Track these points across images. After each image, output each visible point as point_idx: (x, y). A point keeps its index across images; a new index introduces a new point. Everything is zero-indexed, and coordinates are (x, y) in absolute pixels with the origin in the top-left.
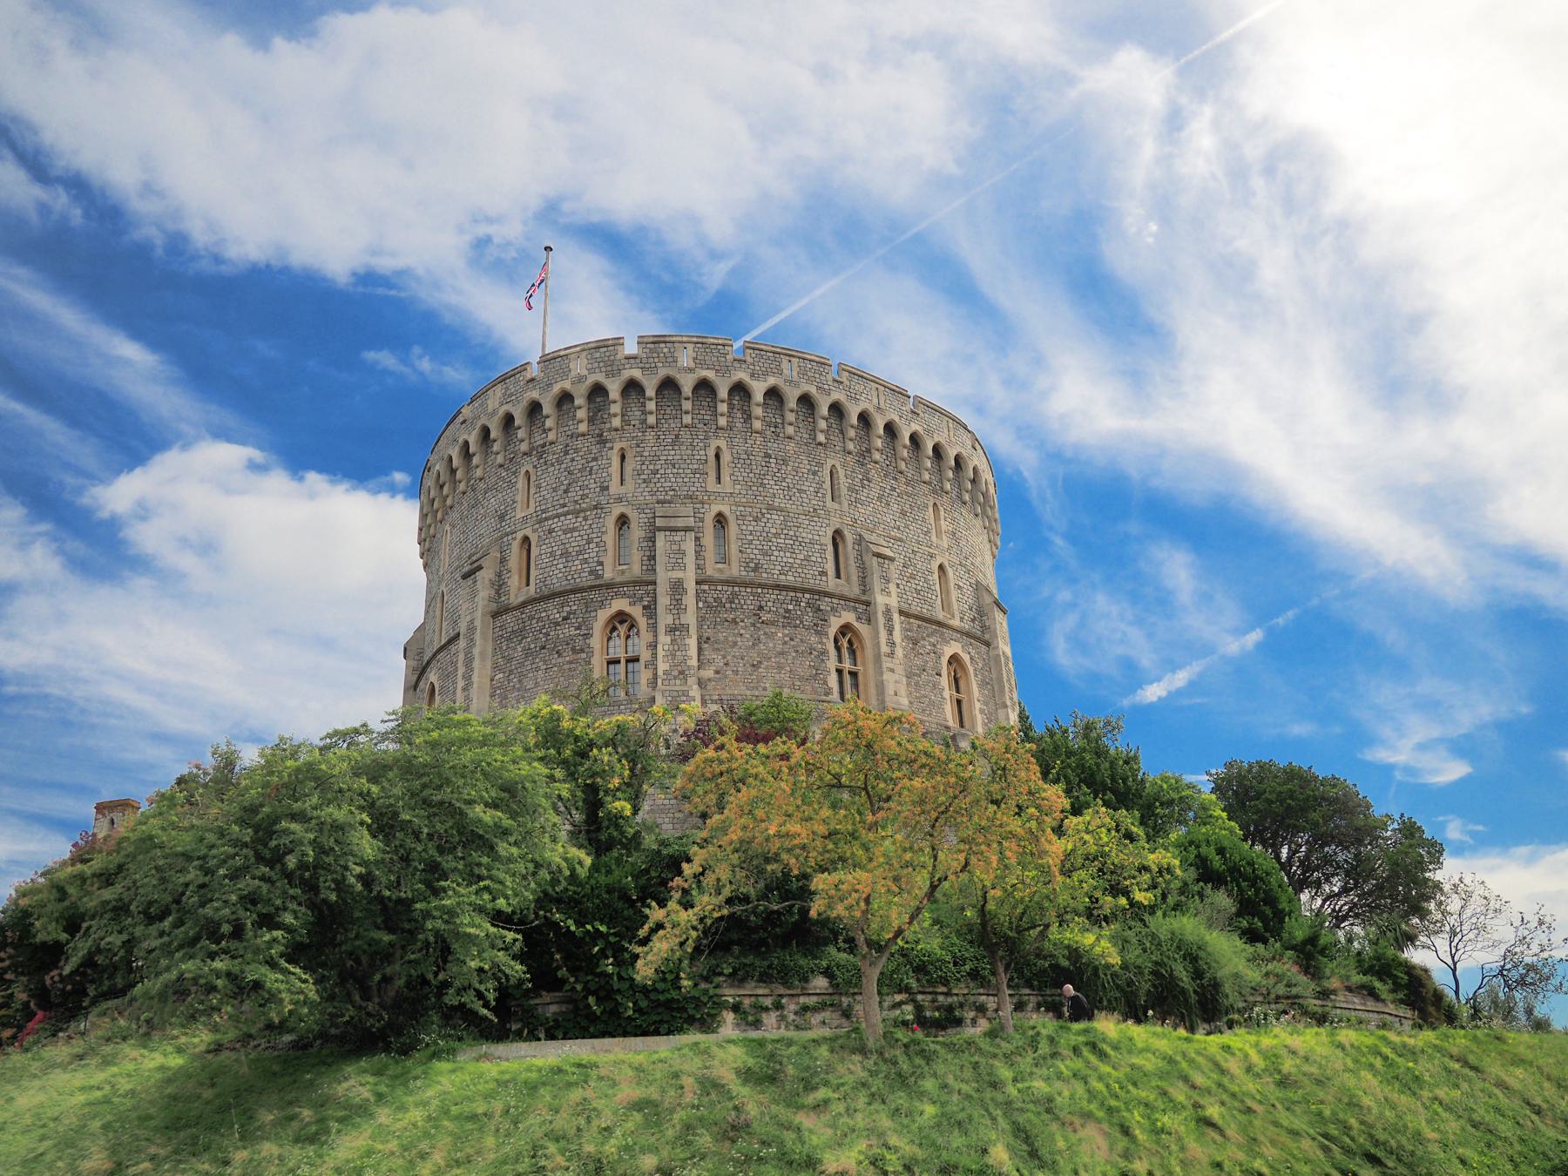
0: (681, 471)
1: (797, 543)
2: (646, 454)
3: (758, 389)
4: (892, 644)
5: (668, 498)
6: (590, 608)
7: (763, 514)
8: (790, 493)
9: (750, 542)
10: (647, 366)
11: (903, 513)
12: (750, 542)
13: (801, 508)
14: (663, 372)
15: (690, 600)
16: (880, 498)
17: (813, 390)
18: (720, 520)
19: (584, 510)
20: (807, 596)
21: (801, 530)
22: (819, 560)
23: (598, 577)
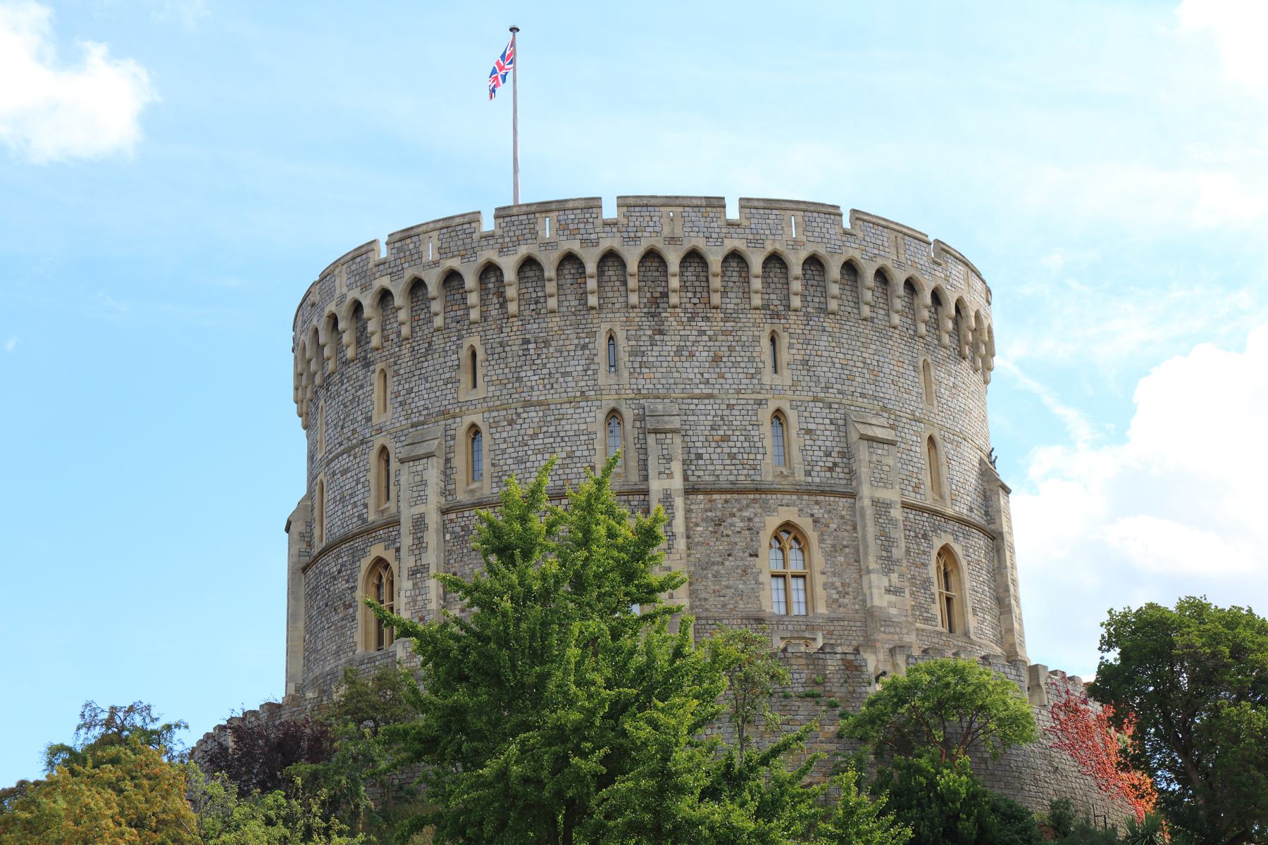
0: (433, 384)
1: (559, 439)
2: (402, 372)
3: (509, 266)
5: (422, 418)
6: (356, 556)
7: (519, 415)
8: (552, 381)
9: (504, 452)
10: (395, 270)
11: (717, 360)
12: (504, 452)
13: (564, 395)
14: (409, 274)
15: (431, 538)
16: (678, 352)
17: (575, 246)
18: (475, 431)
19: (353, 448)
21: (563, 422)
22: (586, 453)
23: (364, 521)
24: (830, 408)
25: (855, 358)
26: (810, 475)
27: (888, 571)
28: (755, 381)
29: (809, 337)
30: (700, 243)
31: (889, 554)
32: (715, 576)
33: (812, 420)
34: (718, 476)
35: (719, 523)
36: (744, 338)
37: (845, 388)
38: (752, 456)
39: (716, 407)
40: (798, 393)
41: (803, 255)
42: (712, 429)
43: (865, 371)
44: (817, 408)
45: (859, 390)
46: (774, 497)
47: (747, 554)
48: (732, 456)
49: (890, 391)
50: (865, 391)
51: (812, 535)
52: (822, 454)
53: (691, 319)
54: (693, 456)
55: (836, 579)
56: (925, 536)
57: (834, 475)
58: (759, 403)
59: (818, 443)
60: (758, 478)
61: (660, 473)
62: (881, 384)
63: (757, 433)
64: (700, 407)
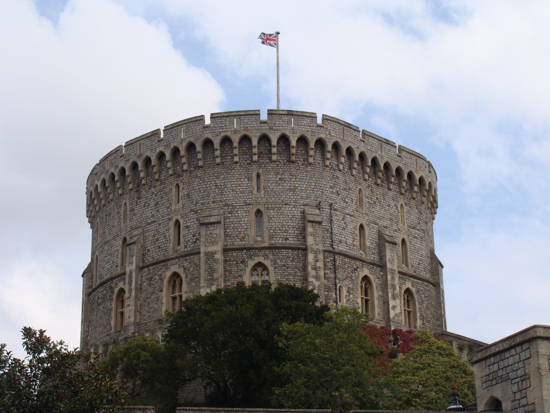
4: (130, 290)
11: (157, 204)
16: (145, 206)
20: (109, 283)
24: (197, 213)
25: (211, 185)
26: (186, 248)
28: (169, 210)
29: (190, 182)
30: (148, 154)
31: (212, 277)
32: (148, 304)
33: (189, 221)
34: (154, 258)
35: (150, 279)
36: (166, 191)
37: (205, 201)
38: (166, 245)
39: (155, 226)
40: (184, 210)
41: (185, 144)
42: (154, 237)
43: (217, 190)
44: (192, 215)
45: (212, 200)
46: (170, 262)
47: (159, 291)
48: (159, 247)
49: (230, 195)
50: (215, 200)
51: (183, 276)
52: (192, 236)
53: (149, 189)
54: (146, 251)
55: (191, 294)
56: (243, 262)
57: (196, 244)
58: (170, 219)
59: (191, 231)
60: (167, 254)
61: (129, 263)
62: (225, 193)
63: (168, 234)
64: (151, 228)
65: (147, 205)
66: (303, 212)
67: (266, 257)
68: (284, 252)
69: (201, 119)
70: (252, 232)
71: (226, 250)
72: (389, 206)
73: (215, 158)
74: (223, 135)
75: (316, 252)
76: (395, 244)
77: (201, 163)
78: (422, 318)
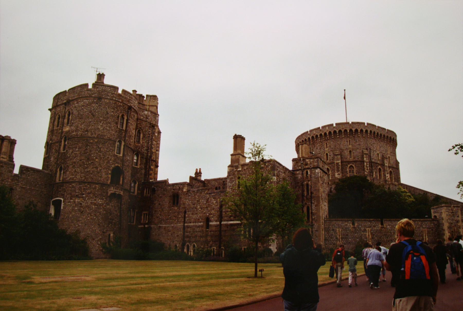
11: (320, 148)
16: (316, 148)
27: (338, 172)
30: (317, 134)
44: (331, 152)
51: (330, 169)
65: (317, 148)
66: (362, 151)
67: (353, 164)
68: (358, 162)
69: (332, 125)
70: (349, 157)
71: (342, 162)
72: (385, 147)
73: (337, 136)
74: (339, 129)
75: (367, 162)
76: (387, 158)
77: (333, 137)
78: (394, 179)
